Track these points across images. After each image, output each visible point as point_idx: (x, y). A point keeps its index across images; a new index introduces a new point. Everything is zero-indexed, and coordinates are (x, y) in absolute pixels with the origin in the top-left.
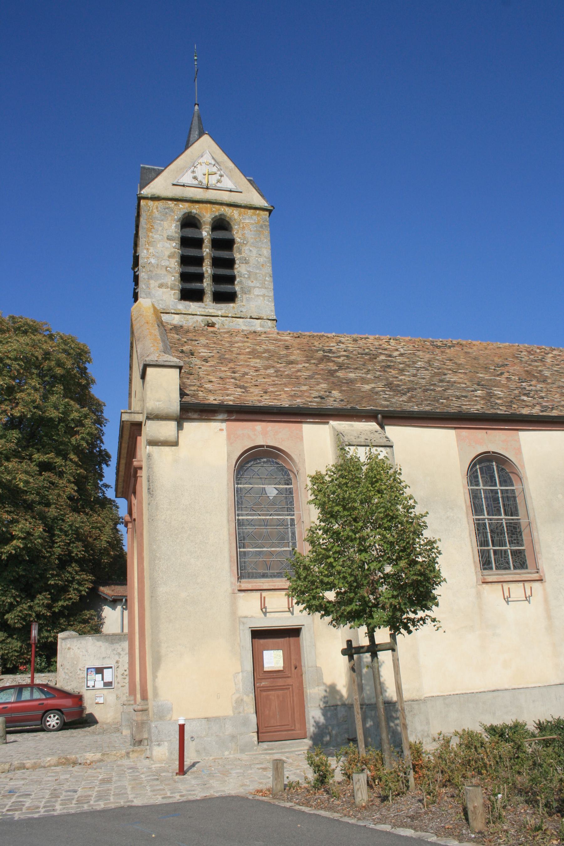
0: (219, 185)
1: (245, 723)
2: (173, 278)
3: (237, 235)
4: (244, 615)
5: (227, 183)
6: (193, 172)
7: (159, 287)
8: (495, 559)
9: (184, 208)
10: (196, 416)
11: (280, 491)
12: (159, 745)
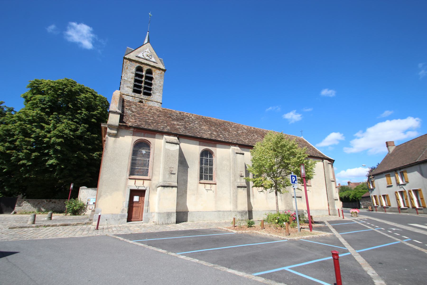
0: (150, 59)
1: (124, 216)
2: (132, 85)
3: (153, 76)
4: (130, 185)
5: (153, 59)
6: (143, 54)
7: (127, 87)
9: (138, 65)
10: (124, 128)
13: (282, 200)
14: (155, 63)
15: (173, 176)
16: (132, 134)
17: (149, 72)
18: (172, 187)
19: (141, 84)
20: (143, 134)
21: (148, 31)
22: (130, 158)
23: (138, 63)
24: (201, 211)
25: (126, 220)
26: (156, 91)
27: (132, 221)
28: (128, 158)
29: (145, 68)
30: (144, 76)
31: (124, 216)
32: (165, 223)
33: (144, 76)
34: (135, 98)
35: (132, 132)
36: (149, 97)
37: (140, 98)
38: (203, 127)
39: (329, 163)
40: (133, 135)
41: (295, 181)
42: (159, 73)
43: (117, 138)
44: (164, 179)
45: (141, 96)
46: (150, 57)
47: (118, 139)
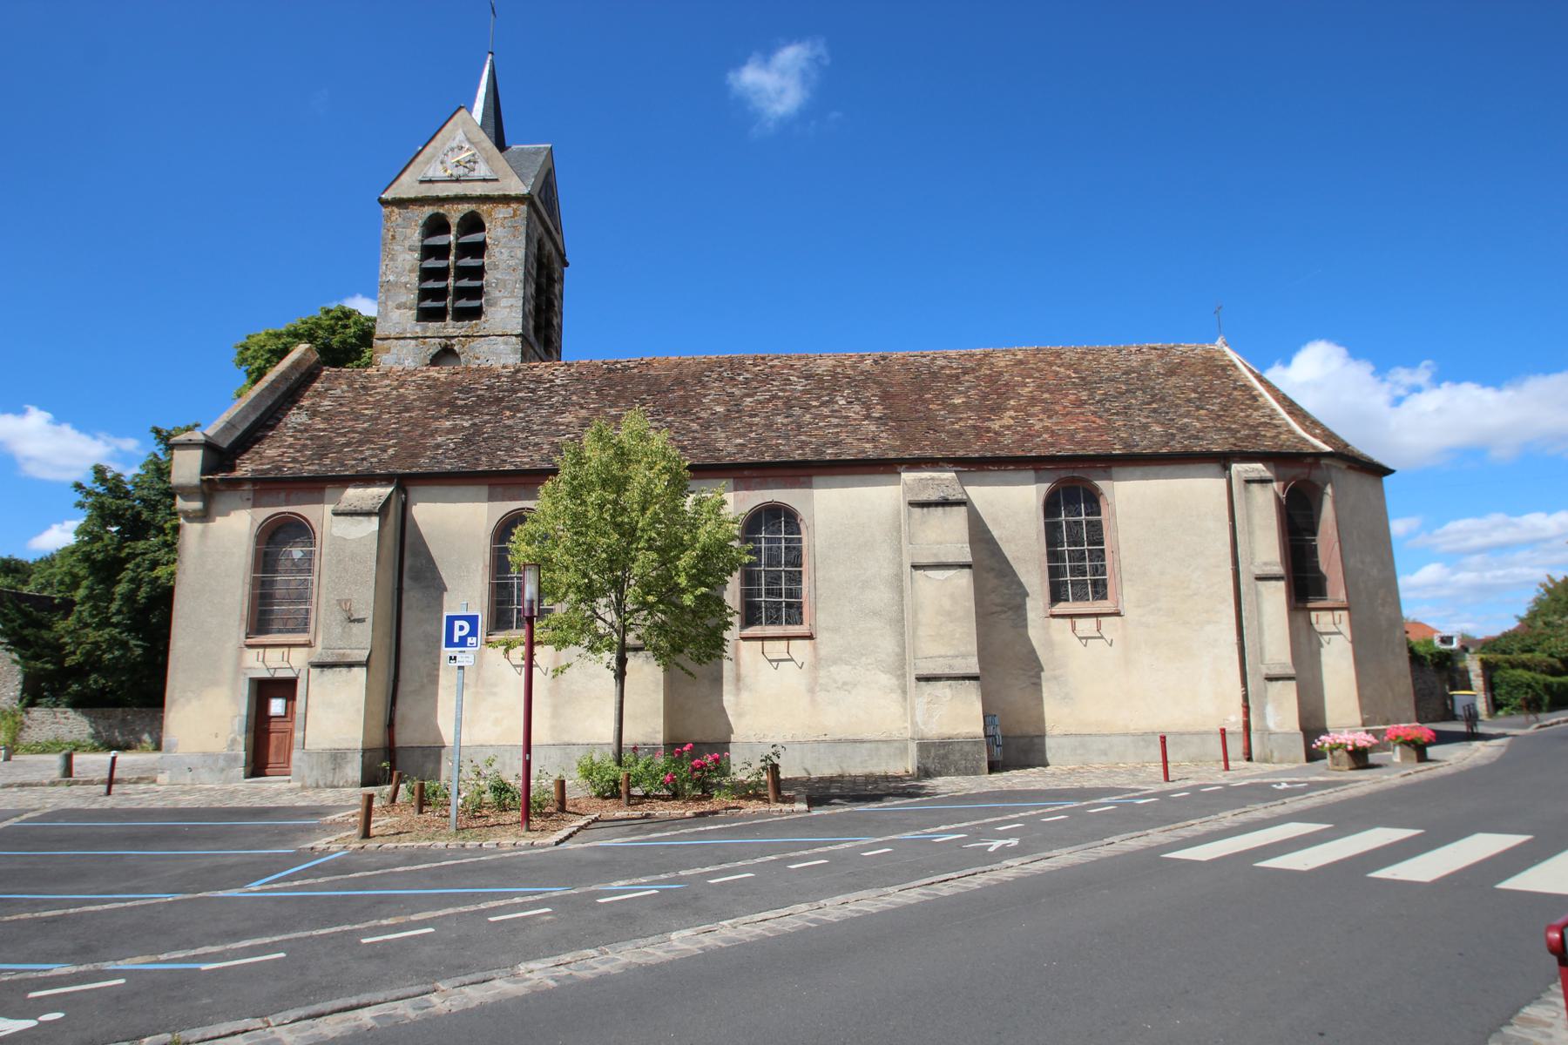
5: (482, 170)
6: (442, 163)
7: (397, 308)
8: (517, 619)
9: (428, 211)
11: (305, 554)
12: (162, 773)
13: (904, 692)
14: (491, 183)
15: (355, 627)
16: (251, 502)
17: (473, 223)
18: (350, 665)
19: (446, 279)
20: (282, 496)
21: (490, 53)
22: (248, 580)
23: (430, 205)
24: (493, 743)
25: (243, 773)
26: (497, 294)
27: (268, 774)
28: (240, 583)
29: (455, 214)
30: (453, 245)
31: (235, 758)
32: (325, 784)
33: (453, 245)
34: (427, 340)
35: (251, 497)
36: (474, 322)
37: (441, 335)
38: (567, 414)
39: (1248, 482)
40: (255, 505)
41: (469, 639)
42: (505, 218)
43: (208, 522)
44: (325, 641)
45: (444, 328)
46: (468, 165)
47: (211, 524)
